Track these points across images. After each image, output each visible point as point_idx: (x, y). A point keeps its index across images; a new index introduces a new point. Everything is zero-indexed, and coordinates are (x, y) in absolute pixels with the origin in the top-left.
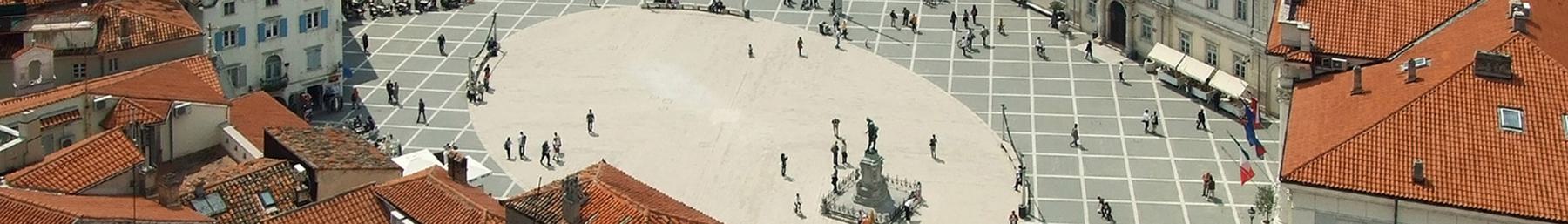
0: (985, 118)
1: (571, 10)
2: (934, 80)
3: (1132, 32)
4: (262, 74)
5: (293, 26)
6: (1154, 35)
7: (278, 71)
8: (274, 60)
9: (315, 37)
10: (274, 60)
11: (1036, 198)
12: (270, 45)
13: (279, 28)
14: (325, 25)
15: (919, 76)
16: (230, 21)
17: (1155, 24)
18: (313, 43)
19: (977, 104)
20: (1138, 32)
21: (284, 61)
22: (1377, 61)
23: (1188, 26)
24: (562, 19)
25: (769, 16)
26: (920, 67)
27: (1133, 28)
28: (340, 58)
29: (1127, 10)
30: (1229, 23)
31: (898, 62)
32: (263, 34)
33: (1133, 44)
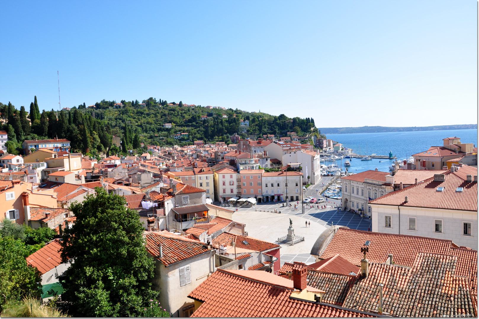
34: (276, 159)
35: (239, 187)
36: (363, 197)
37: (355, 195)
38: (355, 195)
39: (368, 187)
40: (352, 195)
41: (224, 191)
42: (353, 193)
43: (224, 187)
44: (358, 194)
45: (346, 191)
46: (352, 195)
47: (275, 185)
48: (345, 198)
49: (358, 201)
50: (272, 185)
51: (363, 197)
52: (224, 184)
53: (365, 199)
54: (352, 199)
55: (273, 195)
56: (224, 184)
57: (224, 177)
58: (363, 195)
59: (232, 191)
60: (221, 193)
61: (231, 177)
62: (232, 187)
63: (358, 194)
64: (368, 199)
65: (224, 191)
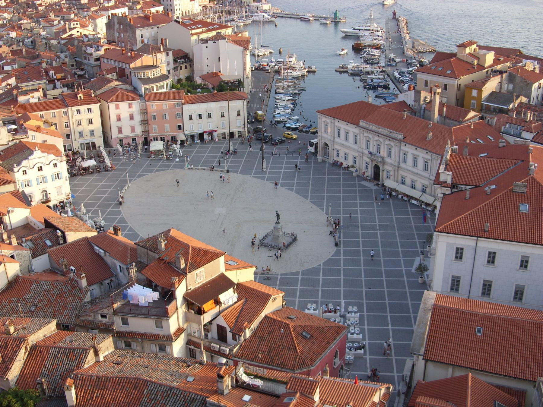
0: (323, 210)
1: (157, 171)
2: (303, 196)
3: (382, 176)
6: (391, 177)
9: (58, 182)
12: (43, 186)
13: (44, 179)
15: (297, 194)
17: (392, 173)
19: (320, 205)
20: (385, 176)
21: (48, 193)
23: (404, 174)
24: (153, 174)
25: (237, 172)
26: (297, 192)
27: (383, 175)
28: (69, 191)
29: (381, 168)
31: (289, 189)
32: (39, 183)
34: (180, 50)
35: (145, 122)
37: (342, 140)
38: (342, 140)
40: (337, 140)
41: (120, 131)
42: (339, 136)
43: (119, 124)
44: (347, 139)
46: (337, 140)
47: (205, 116)
48: (324, 141)
49: (347, 151)
50: (200, 116)
53: (361, 150)
54: (336, 147)
55: (202, 132)
57: (117, 107)
58: (356, 142)
59: (133, 129)
60: (115, 134)
61: (130, 106)
62: (132, 123)
63: (347, 139)
64: (366, 152)
65: (120, 131)
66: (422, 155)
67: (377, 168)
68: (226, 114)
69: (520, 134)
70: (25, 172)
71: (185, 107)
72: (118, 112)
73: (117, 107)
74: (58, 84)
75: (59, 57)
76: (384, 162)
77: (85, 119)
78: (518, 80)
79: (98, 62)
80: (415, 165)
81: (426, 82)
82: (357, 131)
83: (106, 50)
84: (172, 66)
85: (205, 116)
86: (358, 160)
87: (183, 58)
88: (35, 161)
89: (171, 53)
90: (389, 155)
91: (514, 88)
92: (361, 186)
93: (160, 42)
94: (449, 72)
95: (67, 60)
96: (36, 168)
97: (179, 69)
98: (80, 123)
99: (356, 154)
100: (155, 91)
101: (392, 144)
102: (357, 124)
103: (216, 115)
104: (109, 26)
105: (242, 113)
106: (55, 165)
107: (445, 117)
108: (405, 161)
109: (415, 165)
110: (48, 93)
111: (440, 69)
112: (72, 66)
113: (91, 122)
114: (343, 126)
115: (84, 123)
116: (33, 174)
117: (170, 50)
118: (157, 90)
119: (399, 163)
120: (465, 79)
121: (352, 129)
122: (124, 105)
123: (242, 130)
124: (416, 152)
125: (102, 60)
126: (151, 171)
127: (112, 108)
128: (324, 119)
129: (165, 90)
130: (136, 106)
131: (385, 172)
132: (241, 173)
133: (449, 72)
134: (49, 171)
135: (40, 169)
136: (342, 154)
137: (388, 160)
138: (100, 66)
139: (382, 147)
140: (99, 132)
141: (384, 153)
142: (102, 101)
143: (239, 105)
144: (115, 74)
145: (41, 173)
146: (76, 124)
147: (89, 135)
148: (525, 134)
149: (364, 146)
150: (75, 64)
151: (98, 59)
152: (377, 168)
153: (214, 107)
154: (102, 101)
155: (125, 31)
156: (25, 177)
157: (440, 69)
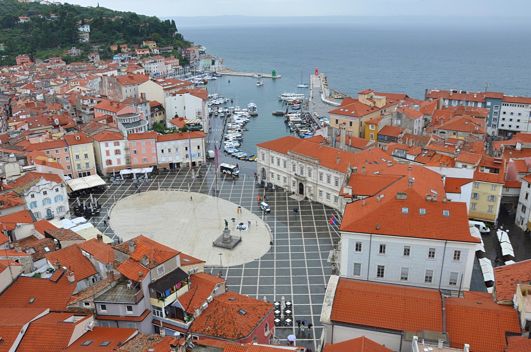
4: (46, 215)
5: (53, 201)
7: (51, 214)
8: (48, 210)
10: (48, 210)
11: (275, 239)
14: (62, 200)
16: (33, 200)
17: (312, 189)
18: (60, 205)
21: (52, 211)
22: (370, 196)
23: (321, 189)
25: (197, 192)
27: (306, 190)
28: (69, 209)
29: (304, 185)
30: (333, 188)
33: (306, 194)
36: (285, 170)
39: (292, 161)
45: (263, 159)
48: (262, 167)
51: (285, 170)
52: (108, 153)
54: (271, 171)
56: (108, 153)
57: (107, 145)
59: (119, 161)
62: (118, 156)
65: (109, 162)
66: (334, 175)
67: (301, 185)
68: (188, 149)
69: (406, 156)
70: (33, 196)
71: (159, 144)
72: (107, 149)
73: (107, 145)
74: (61, 128)
75: (63, 108)
76: (306, 181)
77: (82, 153)
78: (404, 117)
79: (92, 112)
80: (329, 181)
81: (337, 121)
82: (285, 159)
83: (98, 102)
84: (149, 113)
85: (173, 150)
86: (287, 179)
87: (158, 108)
88: (41, 187)
89: (148, 104)
90: (310, 176)
91: (401, 123)
92: (289, 199)
93: (140, 96)
94: (353, 112)
95: (68, 110)
96: (42, 192)
97: (155, 115)
98: (77, 157)
99: (286, 176)
100: (135, 132)
101: (312, 167)
102: (285, 153)
103: (182, 150)
104: (101, 84)
105: (201, 147)
106: (57, 190)
107: (351, 146)
108: (321, 179)
109: (329, 181)
110: (53, 135)
111: (347, 110)
112: (73, 114)
113: (86, 156)
114: (276, 155)
115: (82, 157)
116: (39, 198)
117: (148, 101)
118: (137, 132)
119: (317, 181)
120: (365, 119)
121: (283, 158)
122: (111, 143)
123: (202, 160)
124: (329, 173)
125: (95, 109)
126: (132, 193)
127: (103, 147)
128: (261, 150)
129: (142, 132)
130: (122, 144)
131: (307, 188)
132: (201, 192)
133: (353, 112)
134: (51, 195)
135: (45, 193)
136: (275, 176)
137: (309, 179)
138: (93, 114)
139: (304, 169)
140: (92, 164)
141: (306, 174)
142: (95, 141)
143: (199, 141)
144: (105, 120)
145: (46, 196)
146: (75, 158)
147: (85, 166)
148: (409, 157)
149: (291, 170)
150: (74, 113)
151: (92, 109)
152: (301, 185)
153: (181, 143)
154: (95, 141)
155: (113, 88)
156: (33, 200)
157: (347, 110)
